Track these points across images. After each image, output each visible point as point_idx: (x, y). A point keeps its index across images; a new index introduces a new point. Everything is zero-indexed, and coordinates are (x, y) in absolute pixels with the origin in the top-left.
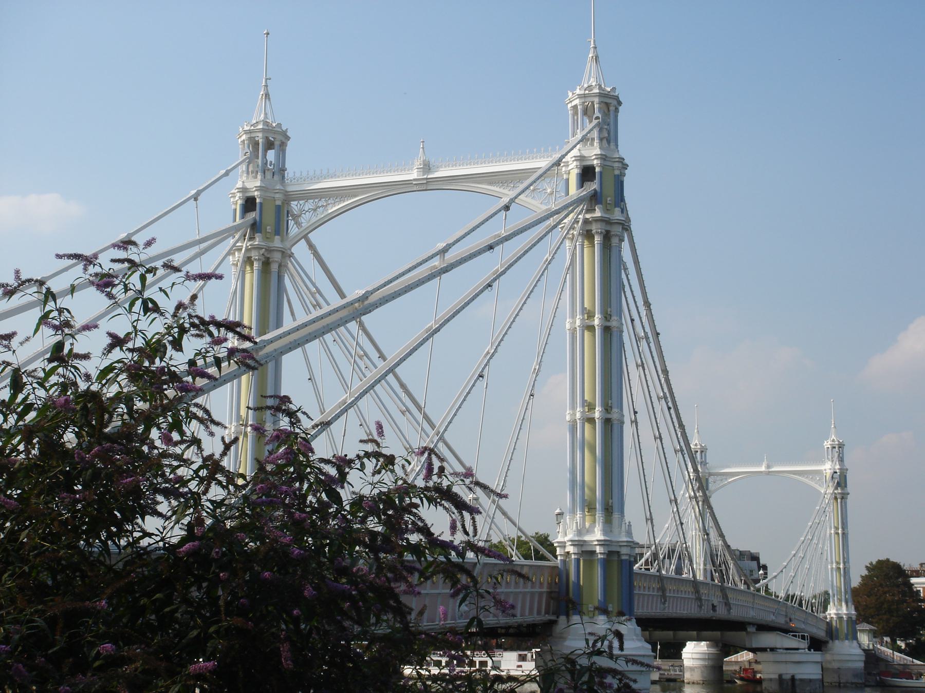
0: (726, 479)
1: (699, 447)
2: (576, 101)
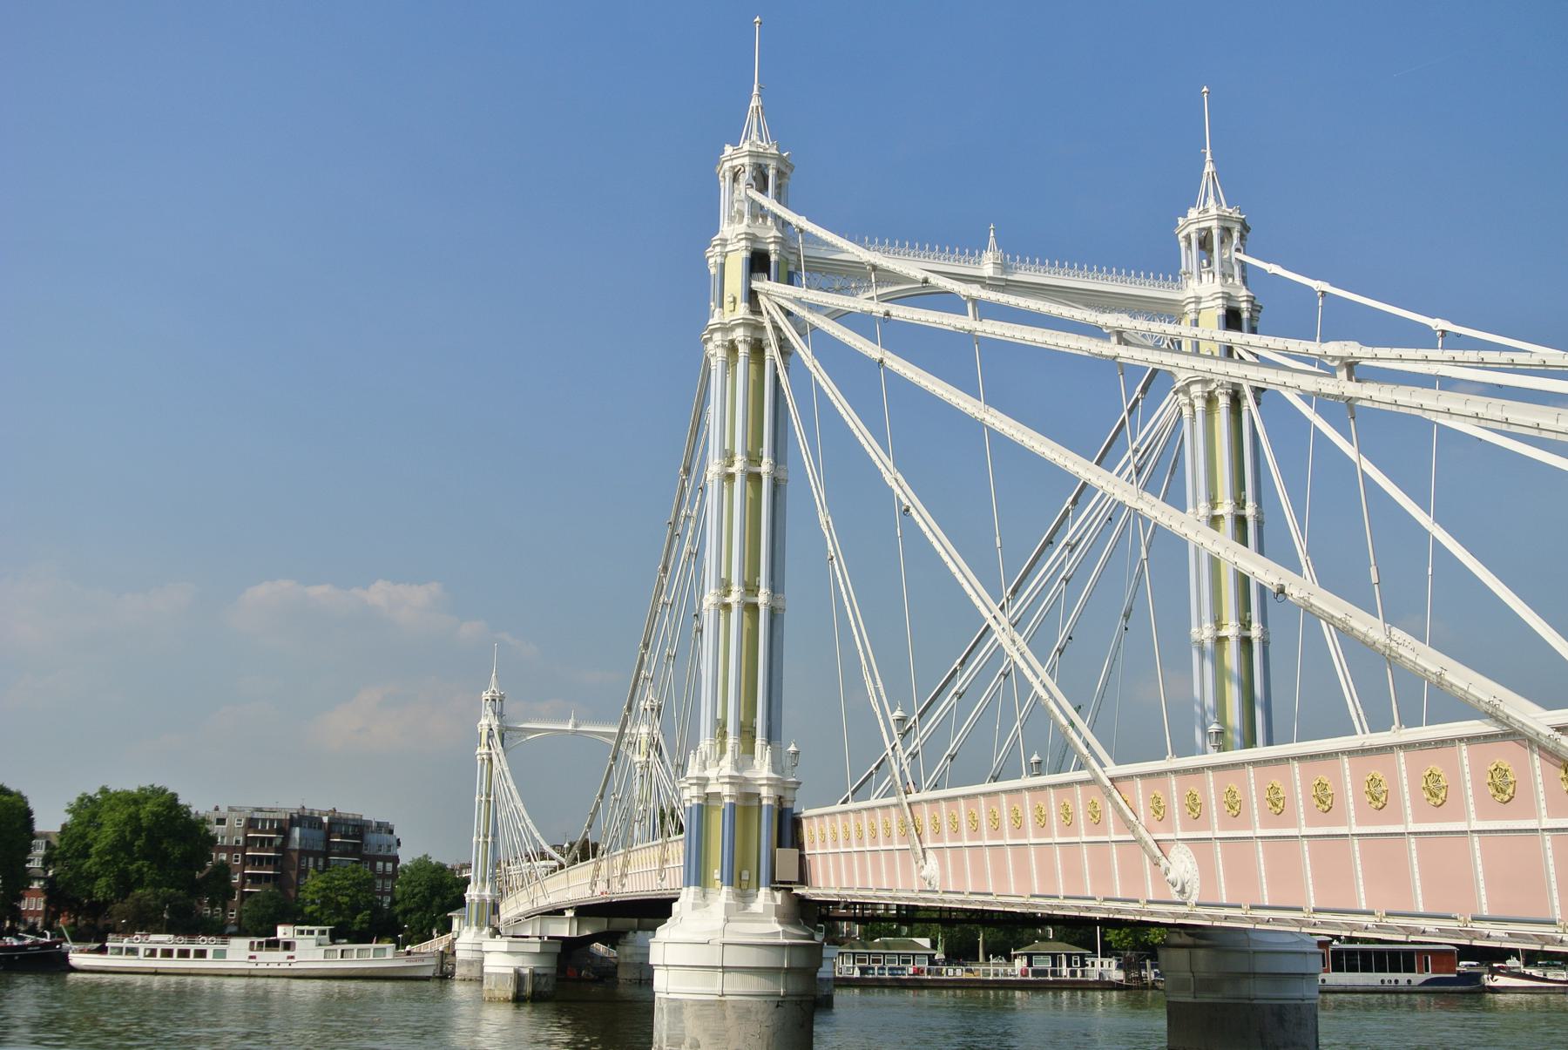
0: (525, 737)
1: (498, 695)
2: (1213, 221)
